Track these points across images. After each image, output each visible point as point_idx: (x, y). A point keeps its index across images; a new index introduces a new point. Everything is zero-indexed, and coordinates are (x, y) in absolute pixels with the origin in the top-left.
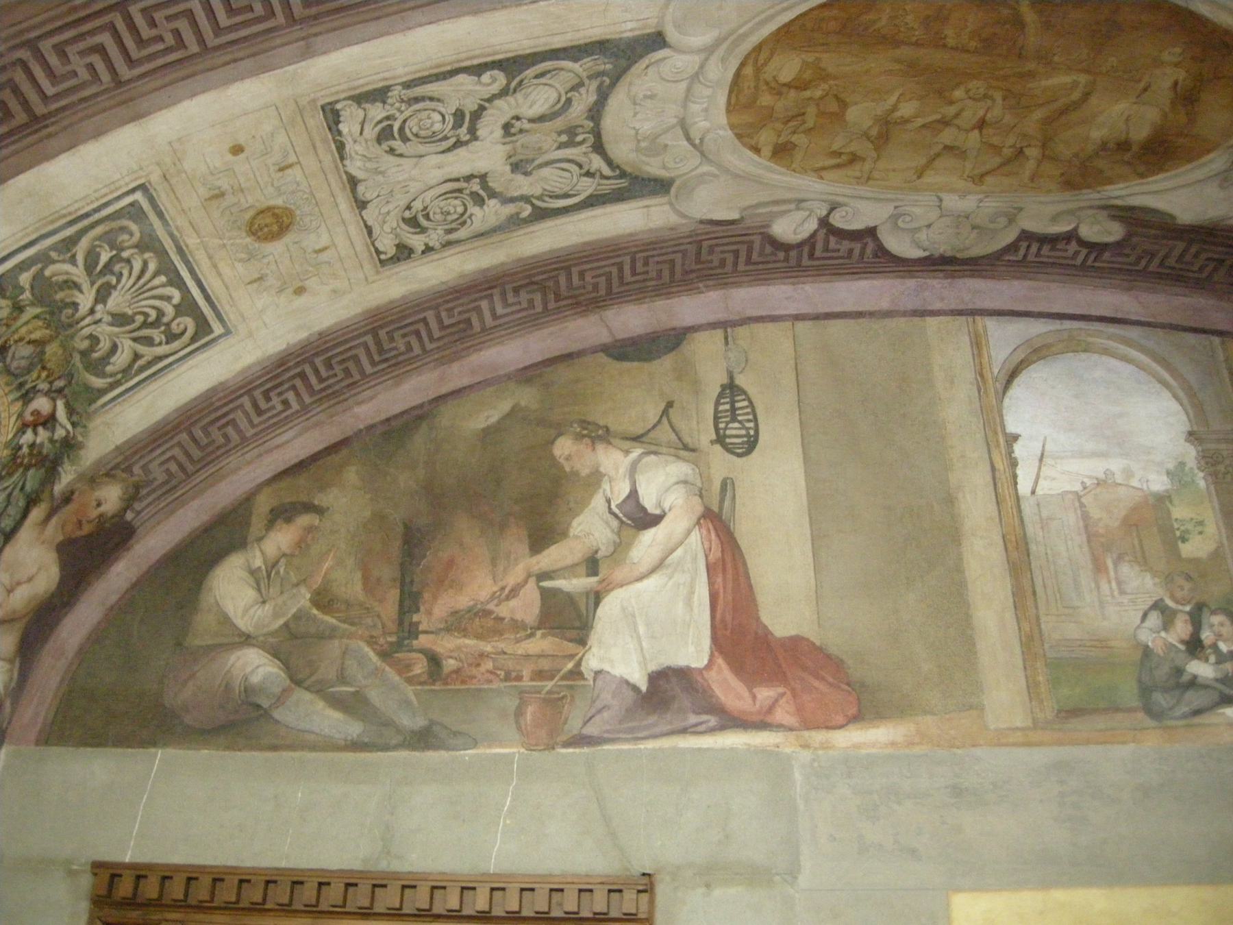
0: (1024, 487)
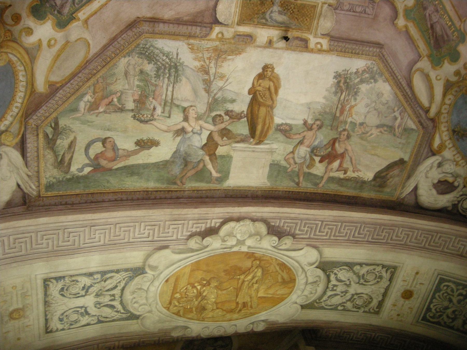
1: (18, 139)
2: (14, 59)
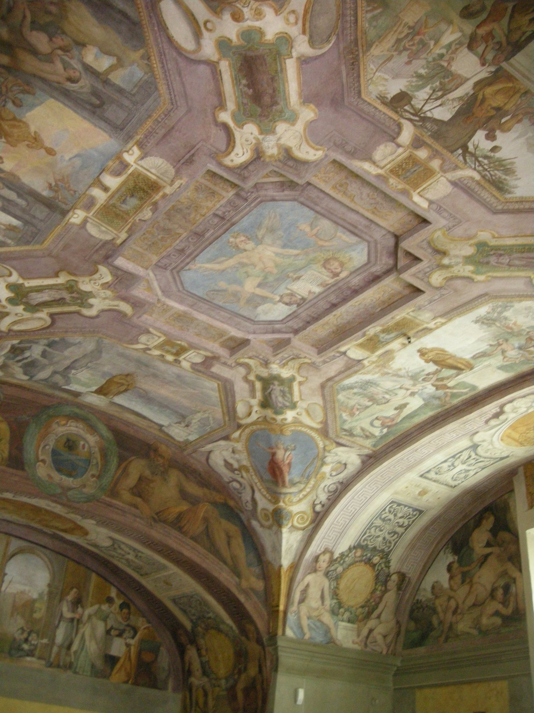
0: (3, 589)
1: (334, 445)
2: (293, 428)
